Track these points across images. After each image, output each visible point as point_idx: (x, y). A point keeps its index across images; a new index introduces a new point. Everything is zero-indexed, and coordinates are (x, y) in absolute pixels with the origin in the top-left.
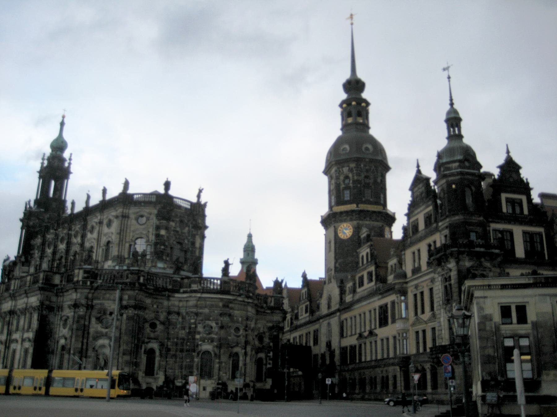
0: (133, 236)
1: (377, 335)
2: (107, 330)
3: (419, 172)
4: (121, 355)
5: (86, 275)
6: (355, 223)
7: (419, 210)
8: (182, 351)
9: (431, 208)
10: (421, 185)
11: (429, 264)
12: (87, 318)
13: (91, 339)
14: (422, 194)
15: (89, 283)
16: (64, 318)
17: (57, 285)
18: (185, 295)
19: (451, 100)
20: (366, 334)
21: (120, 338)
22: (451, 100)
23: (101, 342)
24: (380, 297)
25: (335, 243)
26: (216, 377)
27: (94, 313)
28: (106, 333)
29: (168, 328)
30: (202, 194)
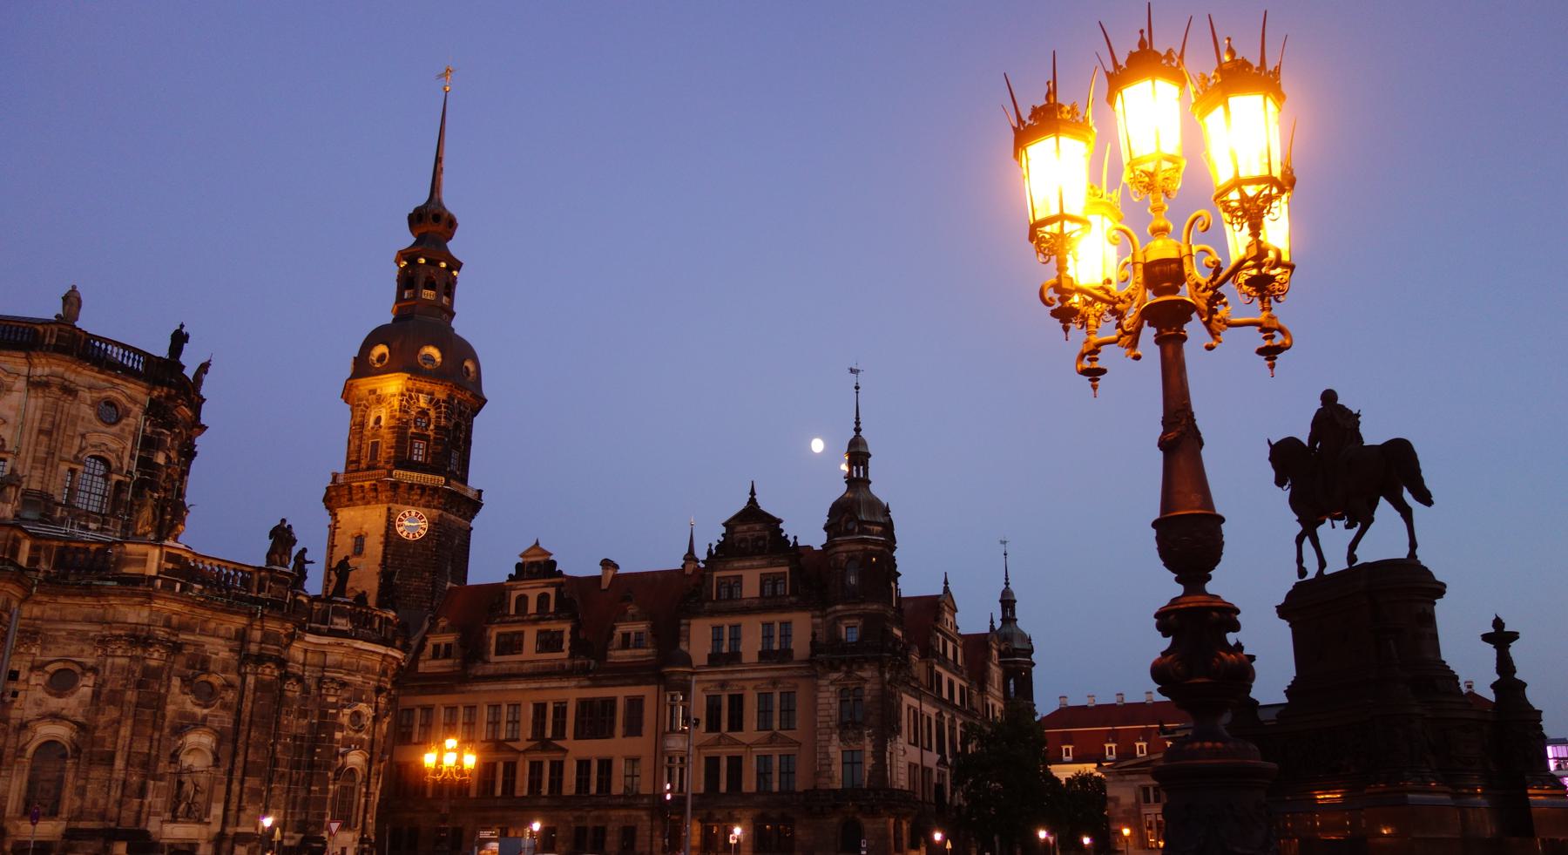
0: (81, 449)
1: (565, 751)
2: (205, 711)
3: (752, 501)
4: (238, 774)
5: (170, 566)
6: (435, 512)
7: (747, 564)
8: (296, 765)
9: (786, 569)
10: (758, 527)
11: (765, 655)
12: (164, 676)
13: (167, 730)
14: (759, 538)
15: (178, 586)
16: (51, 668)
17: (21, 568)
18: (325, 640)
19: (857, 423)
20: (521, 745)
21: (236, 732)
22: (857, 423)
23: (192, 738)
24: (587, 683)
25: (387, 544)
26: (360, 825)
27: (179, 663)
28: (205, 717)
29: (278, 712)
30: (206, 379)
